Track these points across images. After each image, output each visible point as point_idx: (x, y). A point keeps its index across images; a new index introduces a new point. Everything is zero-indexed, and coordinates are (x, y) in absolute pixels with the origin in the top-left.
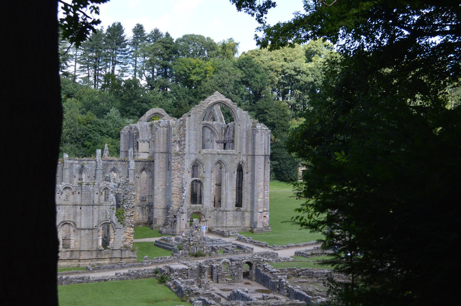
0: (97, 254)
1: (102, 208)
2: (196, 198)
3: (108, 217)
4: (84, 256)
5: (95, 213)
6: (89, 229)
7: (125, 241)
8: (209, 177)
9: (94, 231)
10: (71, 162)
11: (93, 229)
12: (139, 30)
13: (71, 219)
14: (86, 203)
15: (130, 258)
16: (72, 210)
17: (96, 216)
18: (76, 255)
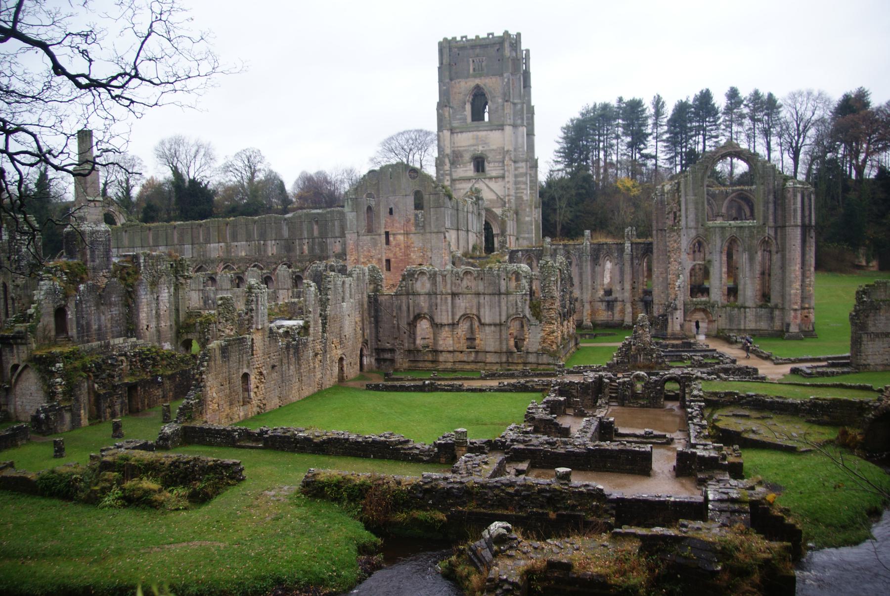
0: (508, 357)
1: (511, 298)
2: (698, 289)
3: (520, 310)
4: (490, 358)
5: (503, 304)
6: (495, 325)
7: (544, 342)
8: (718, 259)
9: (503, 328)
10: (554, 247)
11: (501, 324)
12: (733, 94)
13: (475, 311)
14: (490, 292)
15: (549, 364)
16: (475, 301)
17: (504, 308)
18: (481, 357)
